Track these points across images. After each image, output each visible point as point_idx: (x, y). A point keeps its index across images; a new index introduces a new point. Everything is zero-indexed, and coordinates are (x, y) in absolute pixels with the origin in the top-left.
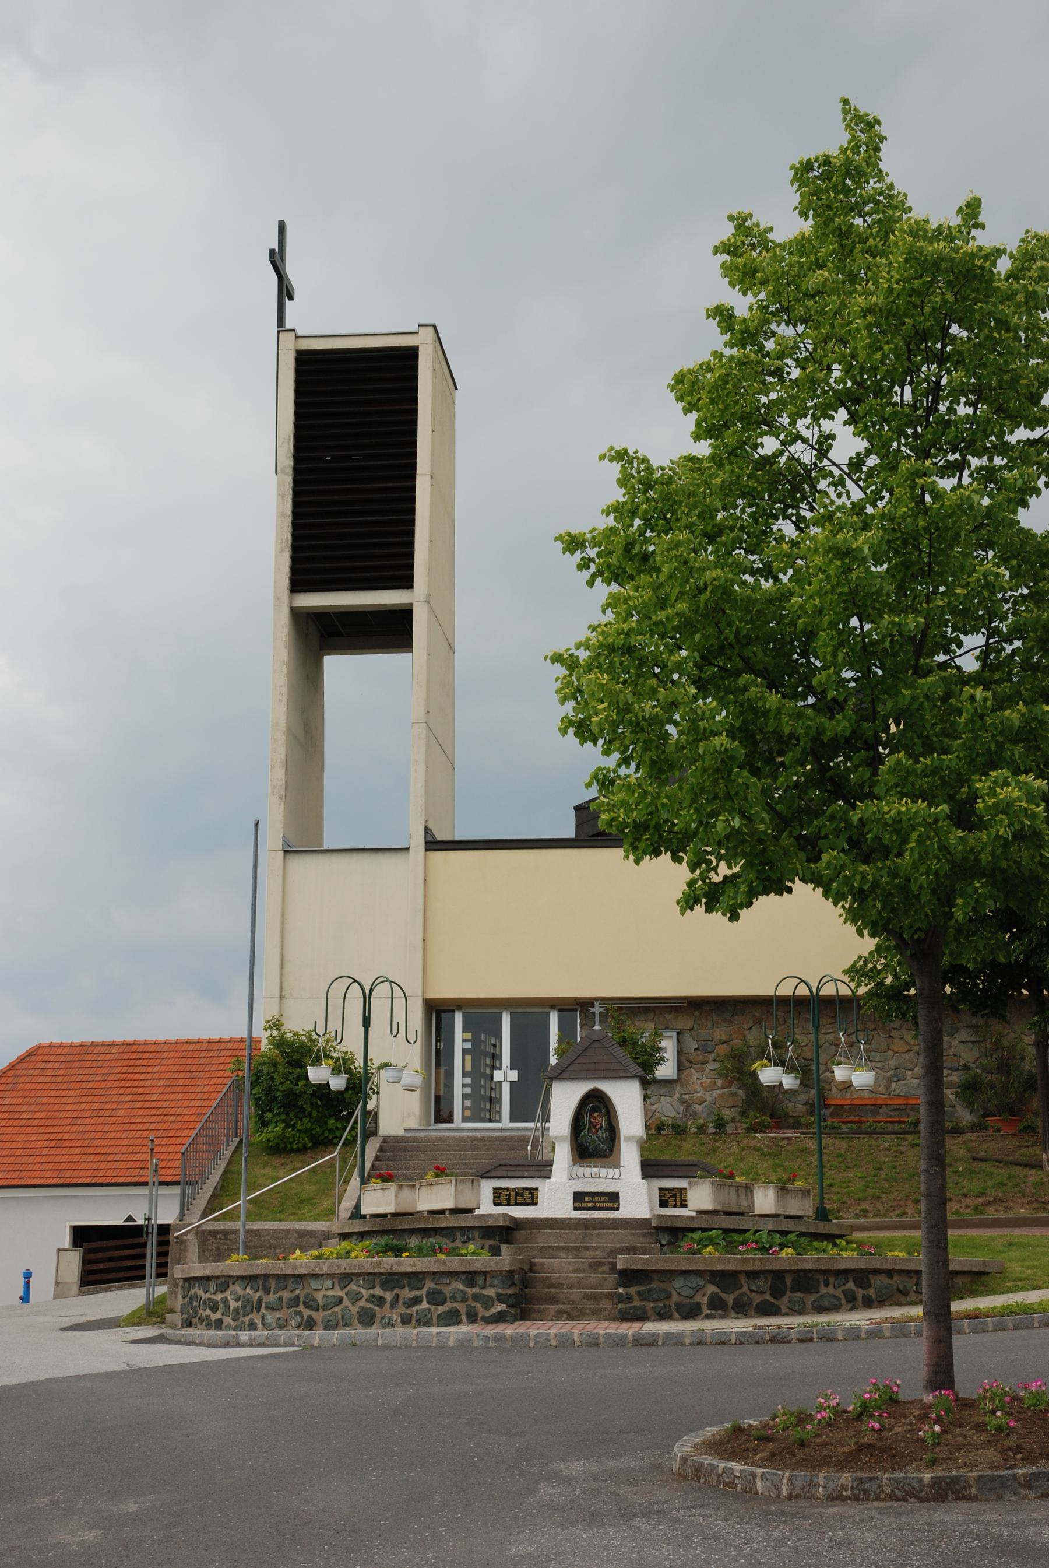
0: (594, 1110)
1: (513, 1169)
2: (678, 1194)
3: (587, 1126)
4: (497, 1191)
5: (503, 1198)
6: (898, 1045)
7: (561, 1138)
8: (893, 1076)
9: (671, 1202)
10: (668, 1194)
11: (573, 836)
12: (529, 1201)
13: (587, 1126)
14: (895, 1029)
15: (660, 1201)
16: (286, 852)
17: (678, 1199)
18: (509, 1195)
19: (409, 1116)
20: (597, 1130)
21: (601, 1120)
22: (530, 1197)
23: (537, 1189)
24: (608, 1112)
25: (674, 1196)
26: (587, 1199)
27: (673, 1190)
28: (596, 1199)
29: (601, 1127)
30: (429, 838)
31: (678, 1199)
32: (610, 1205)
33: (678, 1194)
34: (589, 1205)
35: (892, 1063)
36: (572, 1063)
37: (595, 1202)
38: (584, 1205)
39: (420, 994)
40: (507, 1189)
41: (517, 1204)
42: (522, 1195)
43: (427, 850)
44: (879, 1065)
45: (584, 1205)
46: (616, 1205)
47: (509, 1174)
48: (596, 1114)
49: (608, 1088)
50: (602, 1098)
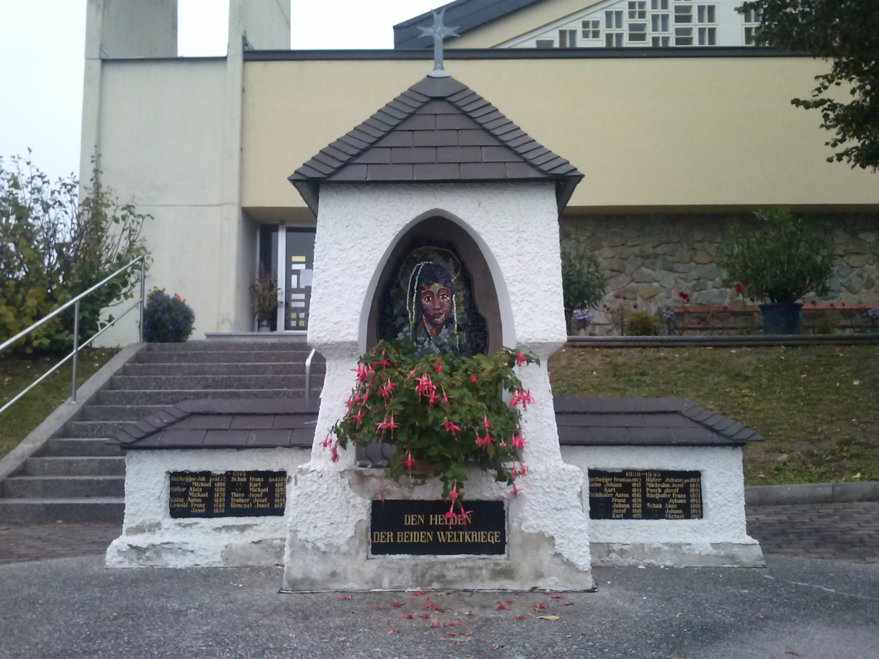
0: (430, 276)
1: (224, 423)
2: (636, 484)
3: (412, 317)
4: (179, 482)
5: (196, 496)
6: (701, 257)
7: (342, 349)
8: (695, 286)
9: (620, 504)
10: (612, 485)
11: (390, 46)
12: (262, 503)
13: (412, 317)
14: (698, 241)
15: (593, 502)
16: (105, 61)
17: (637, 495)
18: (211, 490)
19: (223, 322)
20: (438, 328)
21: (446, 301)
22: (263, 495)
23: (282, 474)
24: (467, 281)
25: (627, 488)
26: (410, 520)
27: (623, 473)
28: (436, 519)
29: (449, 321)
30: (247, 49)
31: (637, 495)
32: (478, 537)
33: (636, 484)
34: (417, 537)
35: (694, 274)
36: (372, 145)
37: (435, 529)
38: (402, 537)
39: (236, 200)
40: (207, 474)
41: (230, 512)
42: (244, 488)
43: (246, 60)
44: (682, 276)
45: (402, 537)
46: (494, 539)
47: (209, 440)
48: (436, 287)
49: (473, 212)
50: (451, 245)
